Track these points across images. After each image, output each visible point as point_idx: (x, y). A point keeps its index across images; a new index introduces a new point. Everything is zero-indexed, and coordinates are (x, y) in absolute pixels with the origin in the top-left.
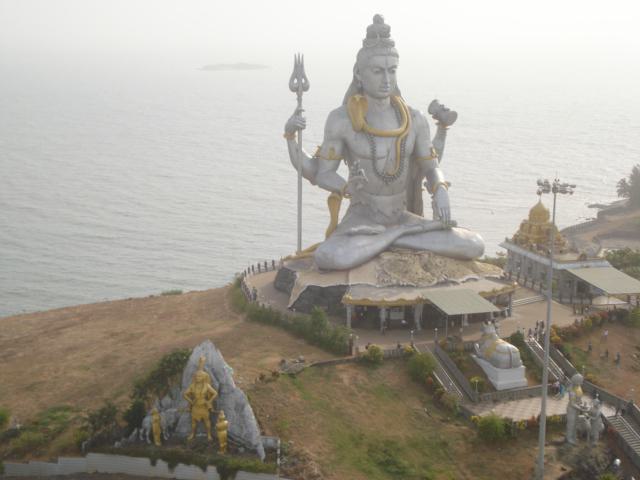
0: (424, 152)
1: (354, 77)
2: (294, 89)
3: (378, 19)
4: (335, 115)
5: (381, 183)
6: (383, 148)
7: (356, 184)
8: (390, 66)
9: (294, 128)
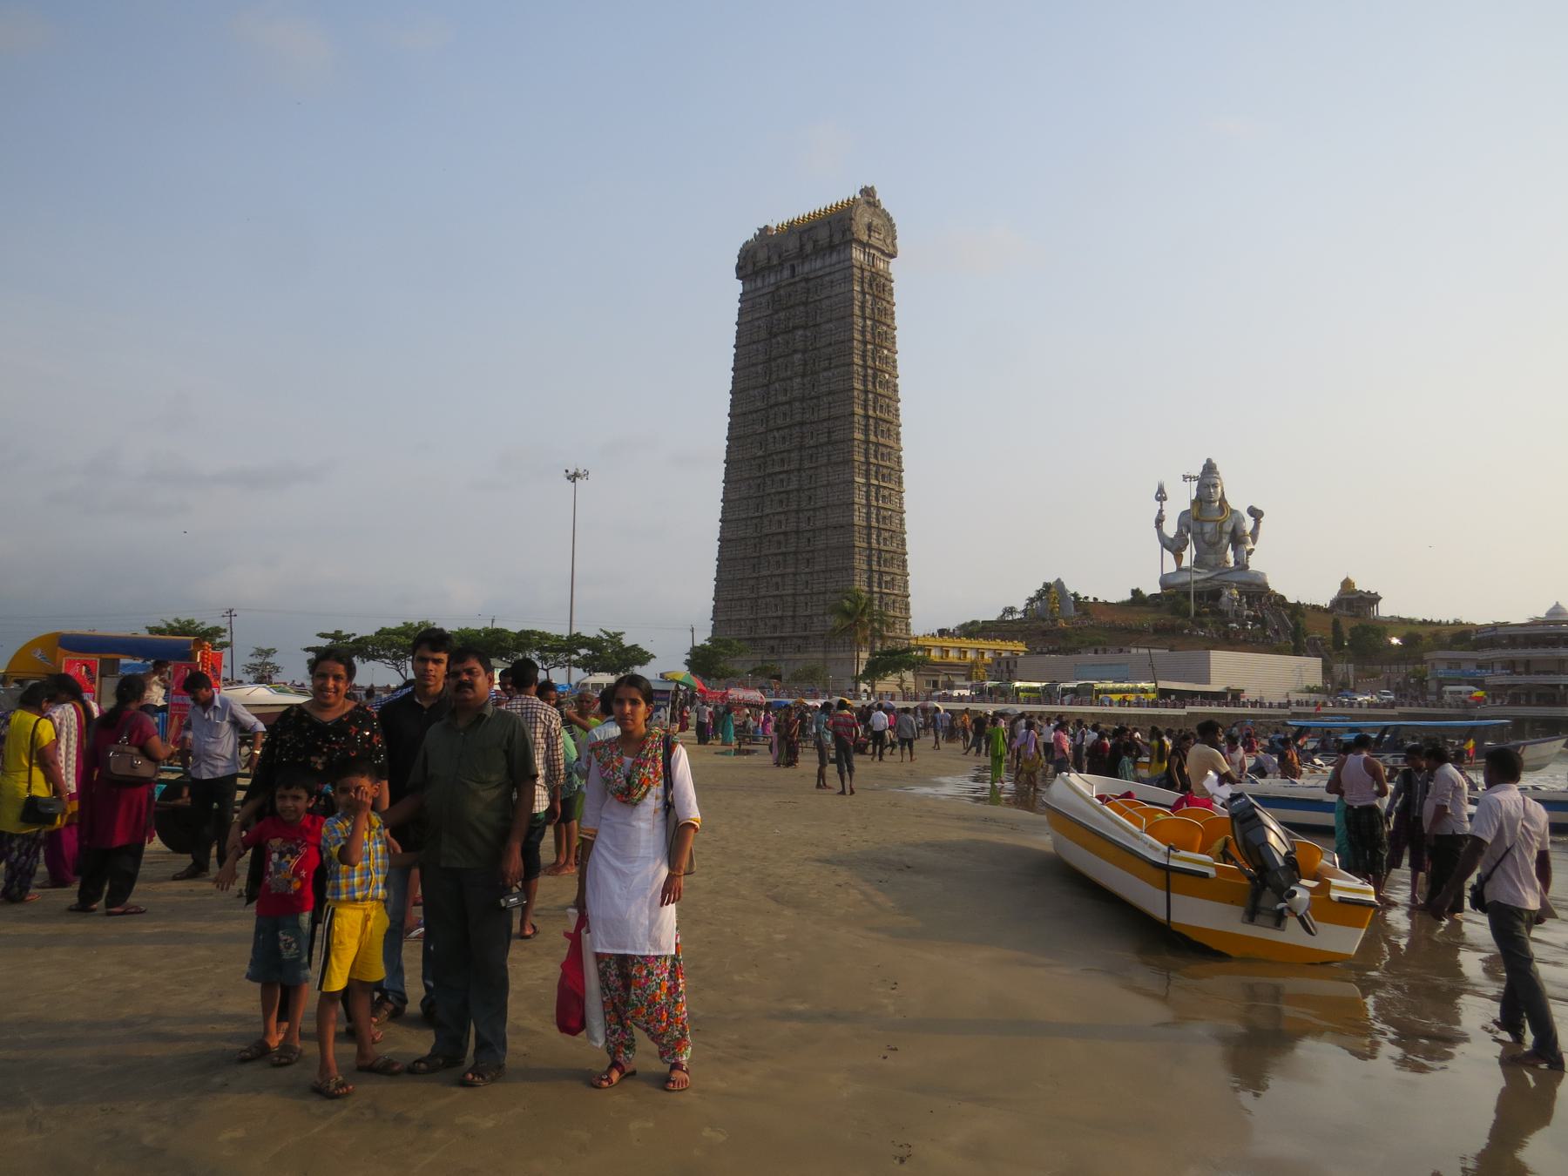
2: (1158, 499)
3: (1209, 461)
4: (1184, 513)
6: (1208, 528)
9: (1159, 521)
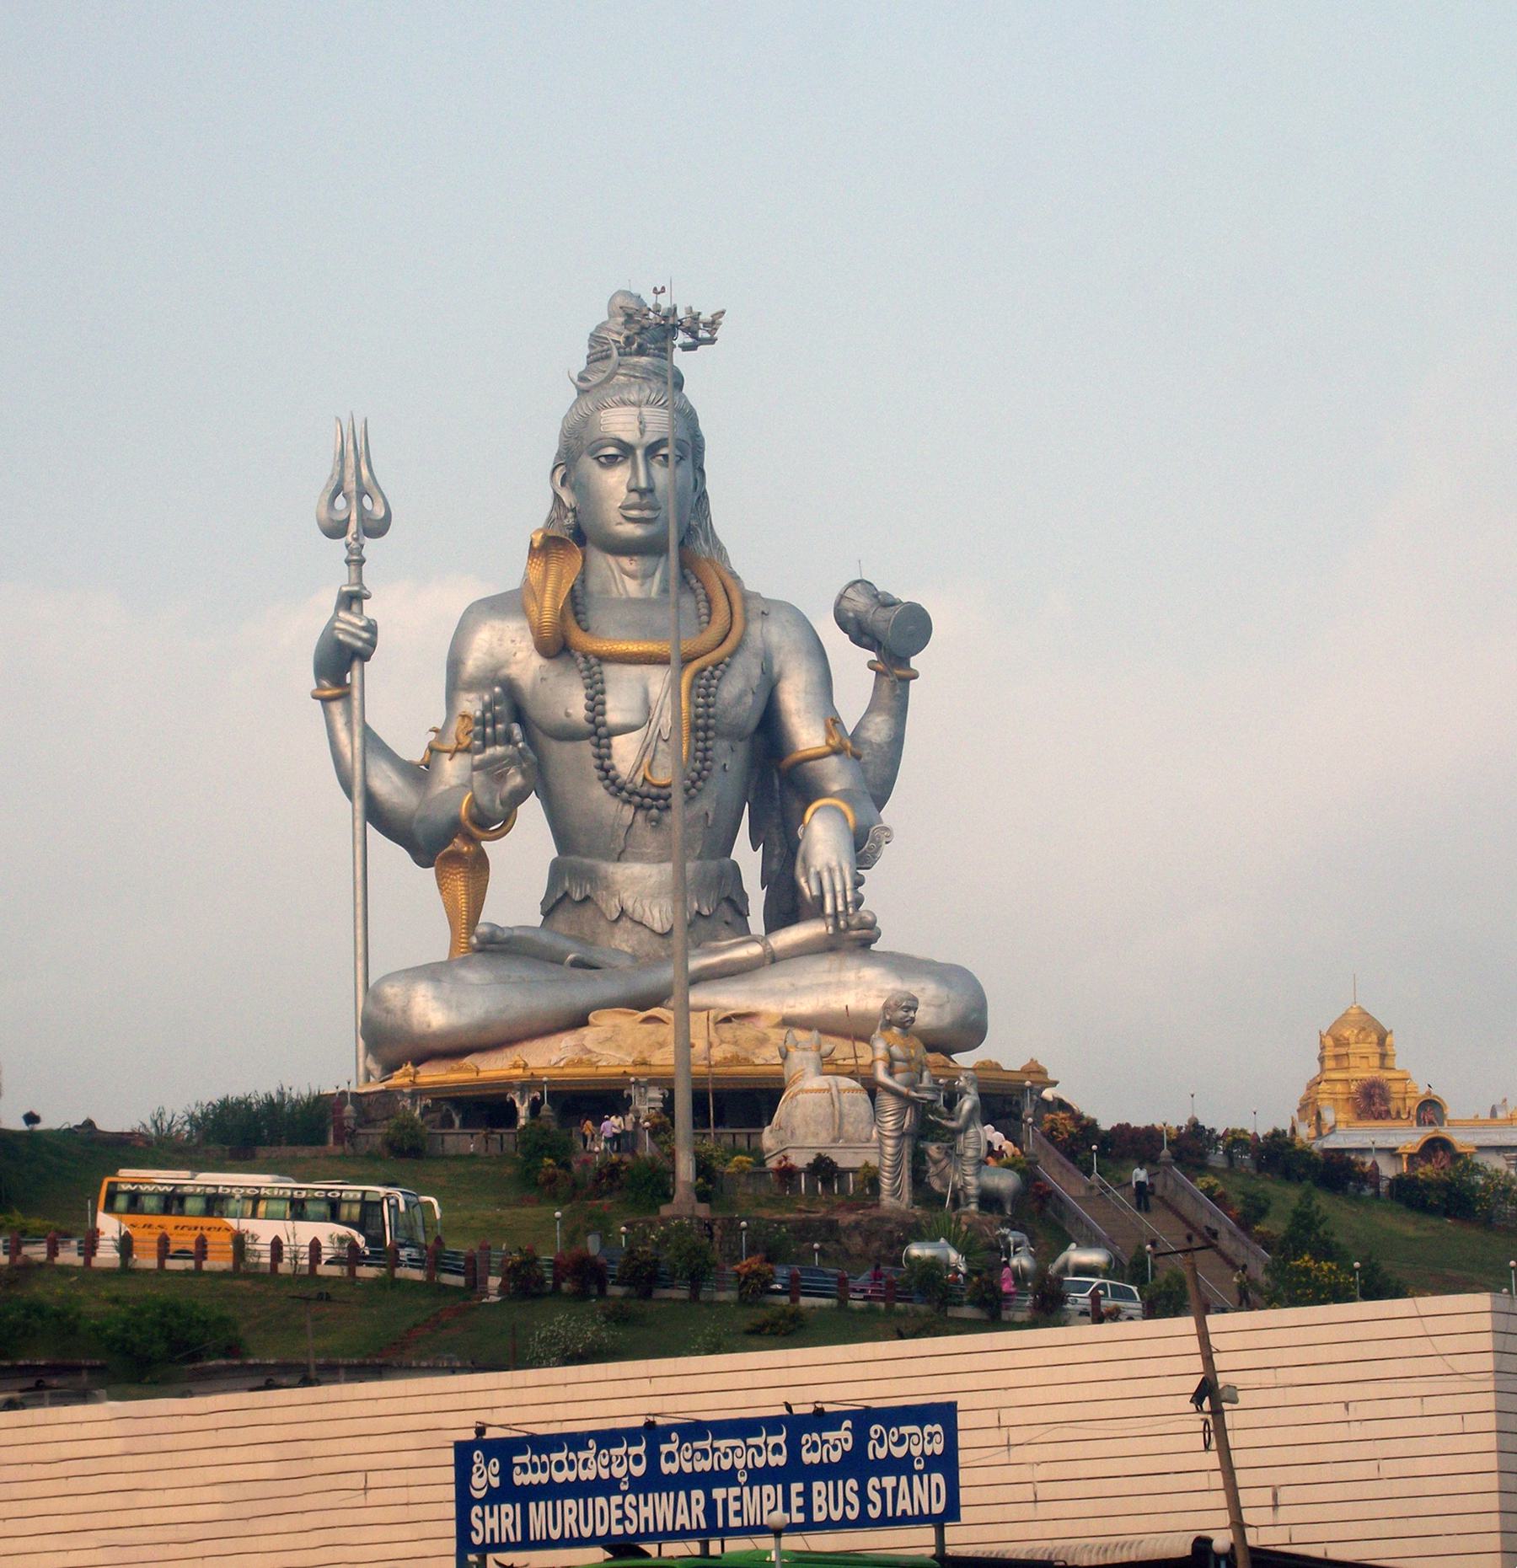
0: (807, 735)
1: (557, 497)
2: (335, 530)
5: (628, 812)
7: (502, 778)
8: (650, 438)
9: (340, 663)
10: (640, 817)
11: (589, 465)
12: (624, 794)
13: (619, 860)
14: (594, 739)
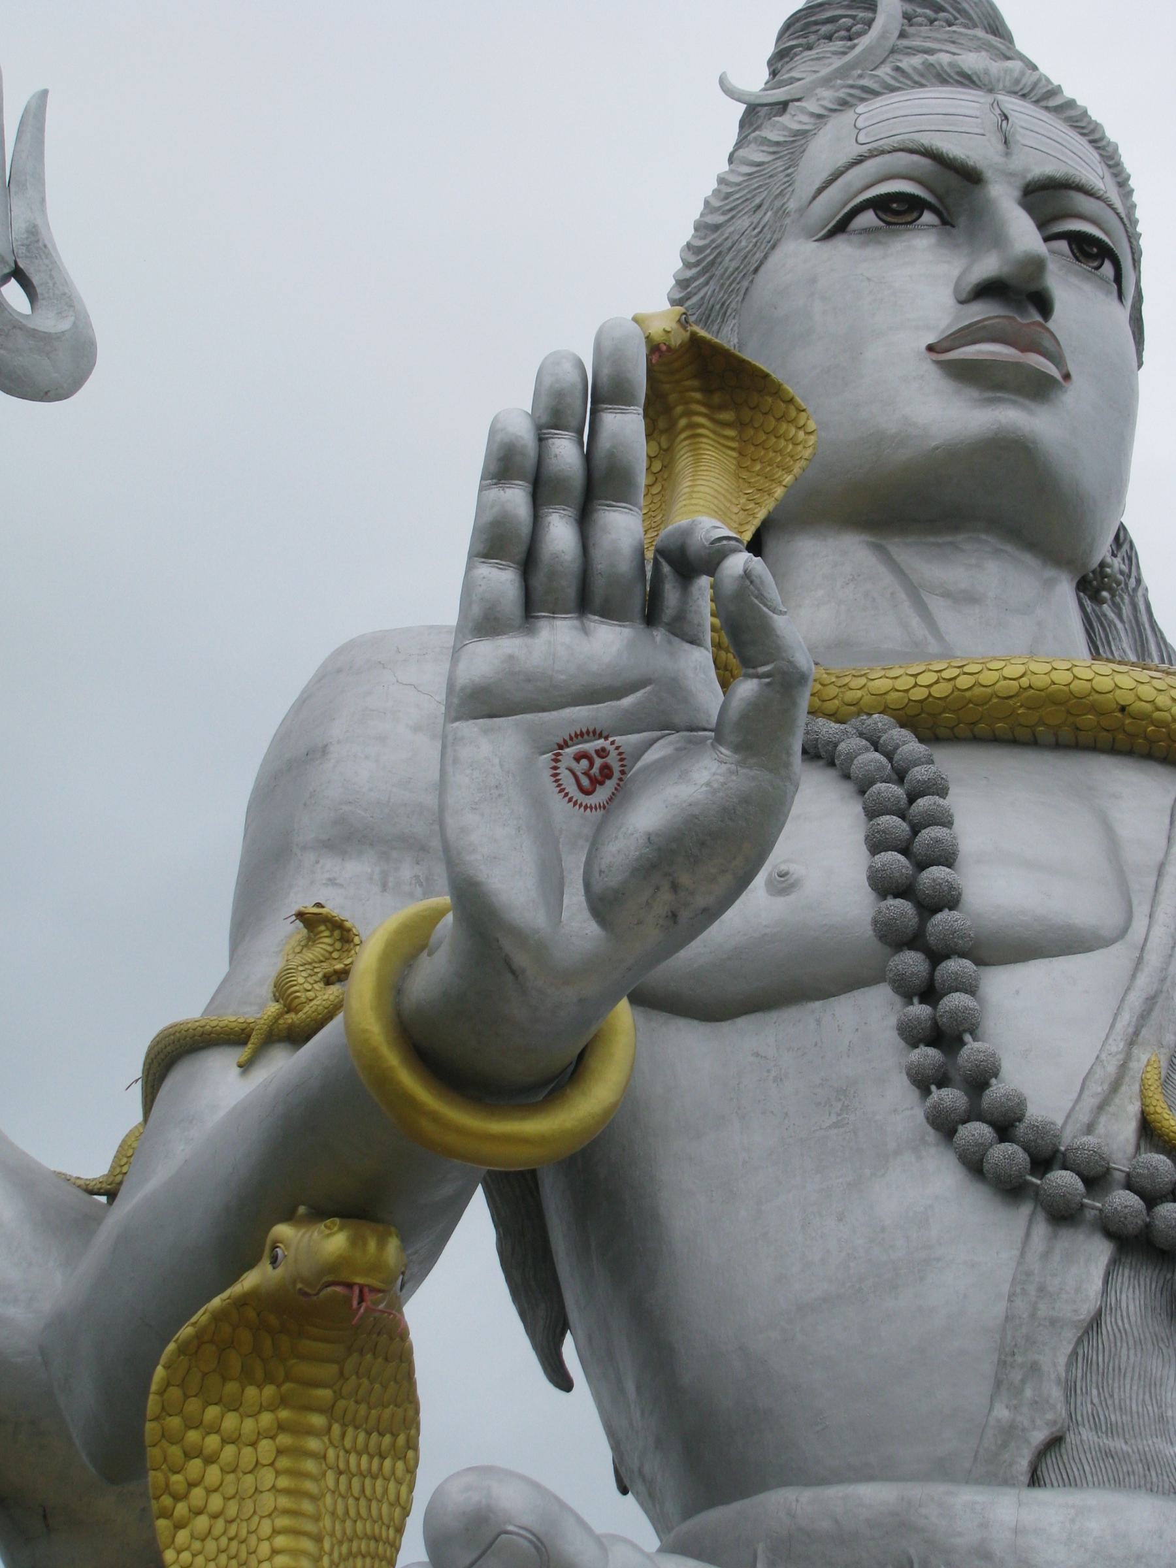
7: (602, 777)
10: (1135, 1297)
11: (798, 259)
12: (1063, 1180)
13: (1035, 1480)
14: (912, 962)
